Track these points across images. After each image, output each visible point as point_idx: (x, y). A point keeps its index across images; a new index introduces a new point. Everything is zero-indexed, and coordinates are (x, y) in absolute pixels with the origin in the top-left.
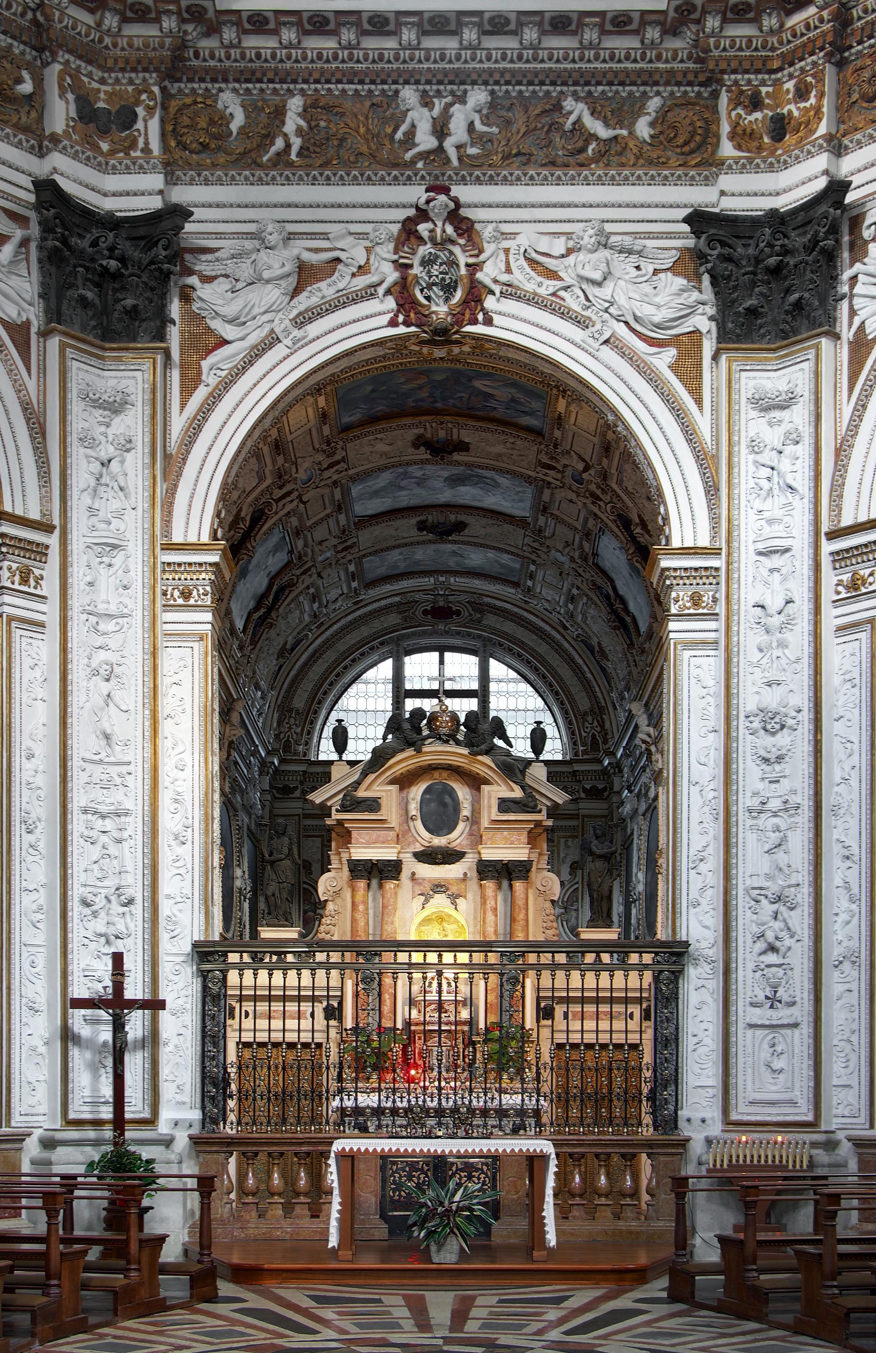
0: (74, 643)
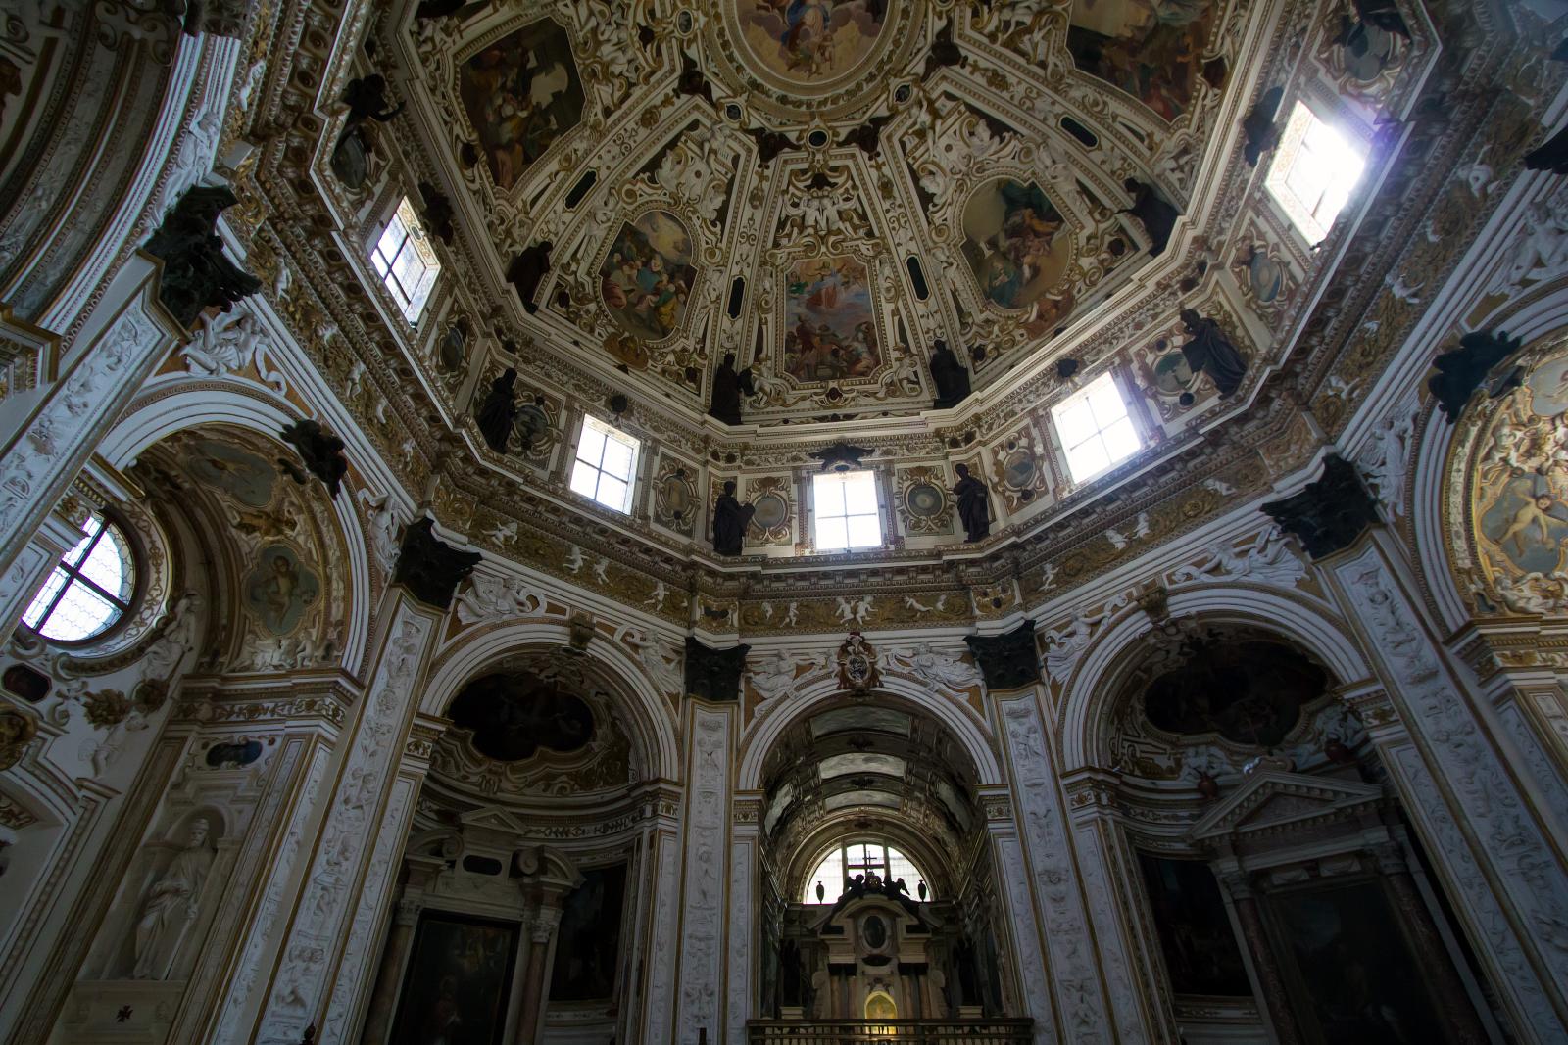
0: (690, 843)
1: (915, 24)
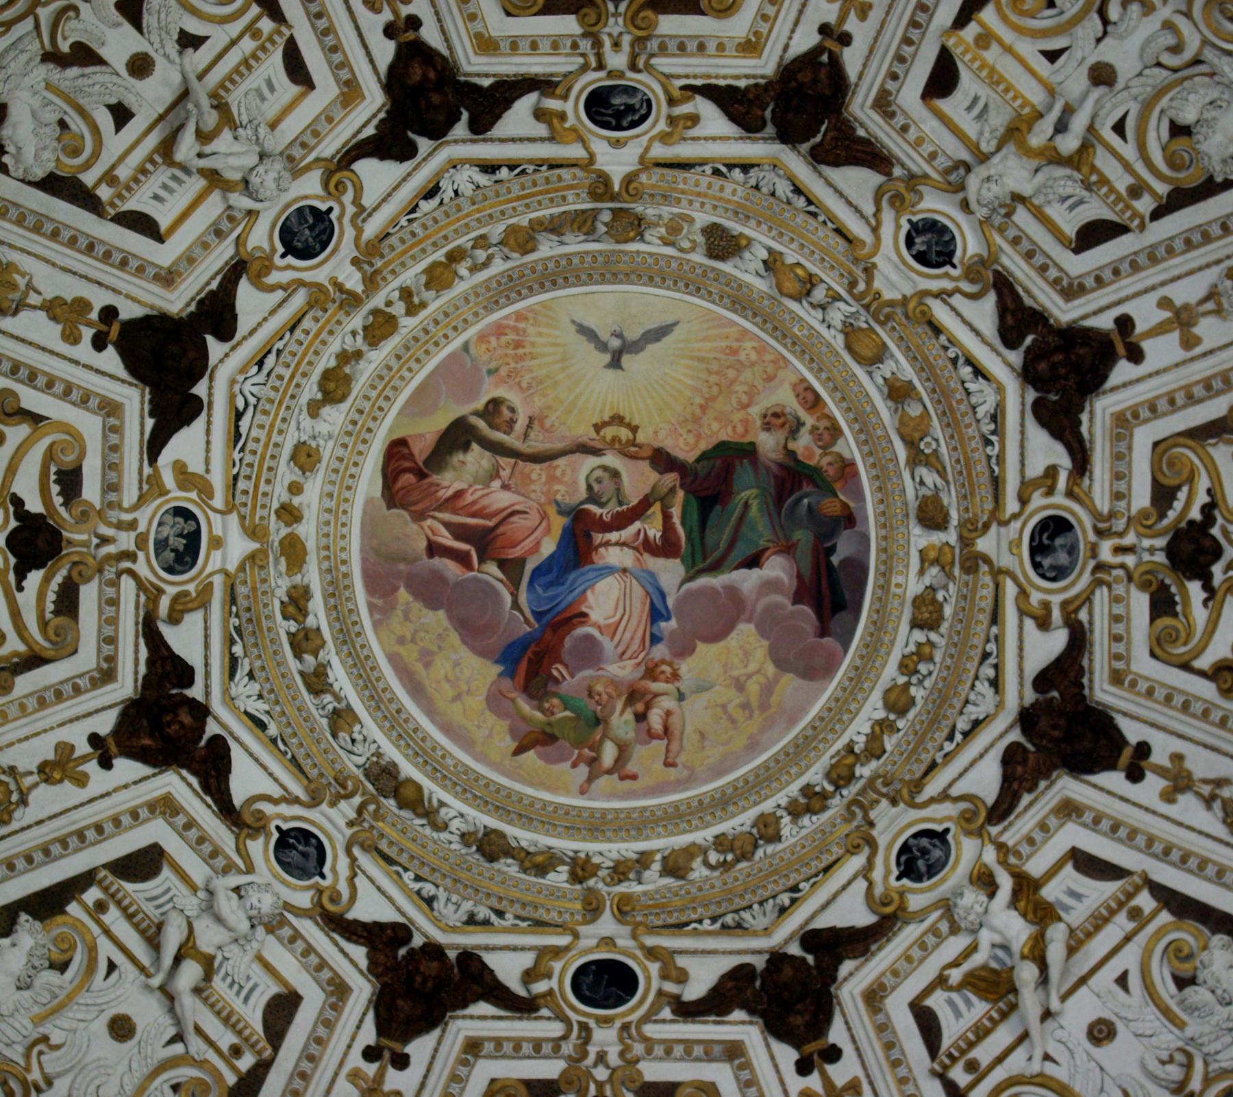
1: (959, 646)
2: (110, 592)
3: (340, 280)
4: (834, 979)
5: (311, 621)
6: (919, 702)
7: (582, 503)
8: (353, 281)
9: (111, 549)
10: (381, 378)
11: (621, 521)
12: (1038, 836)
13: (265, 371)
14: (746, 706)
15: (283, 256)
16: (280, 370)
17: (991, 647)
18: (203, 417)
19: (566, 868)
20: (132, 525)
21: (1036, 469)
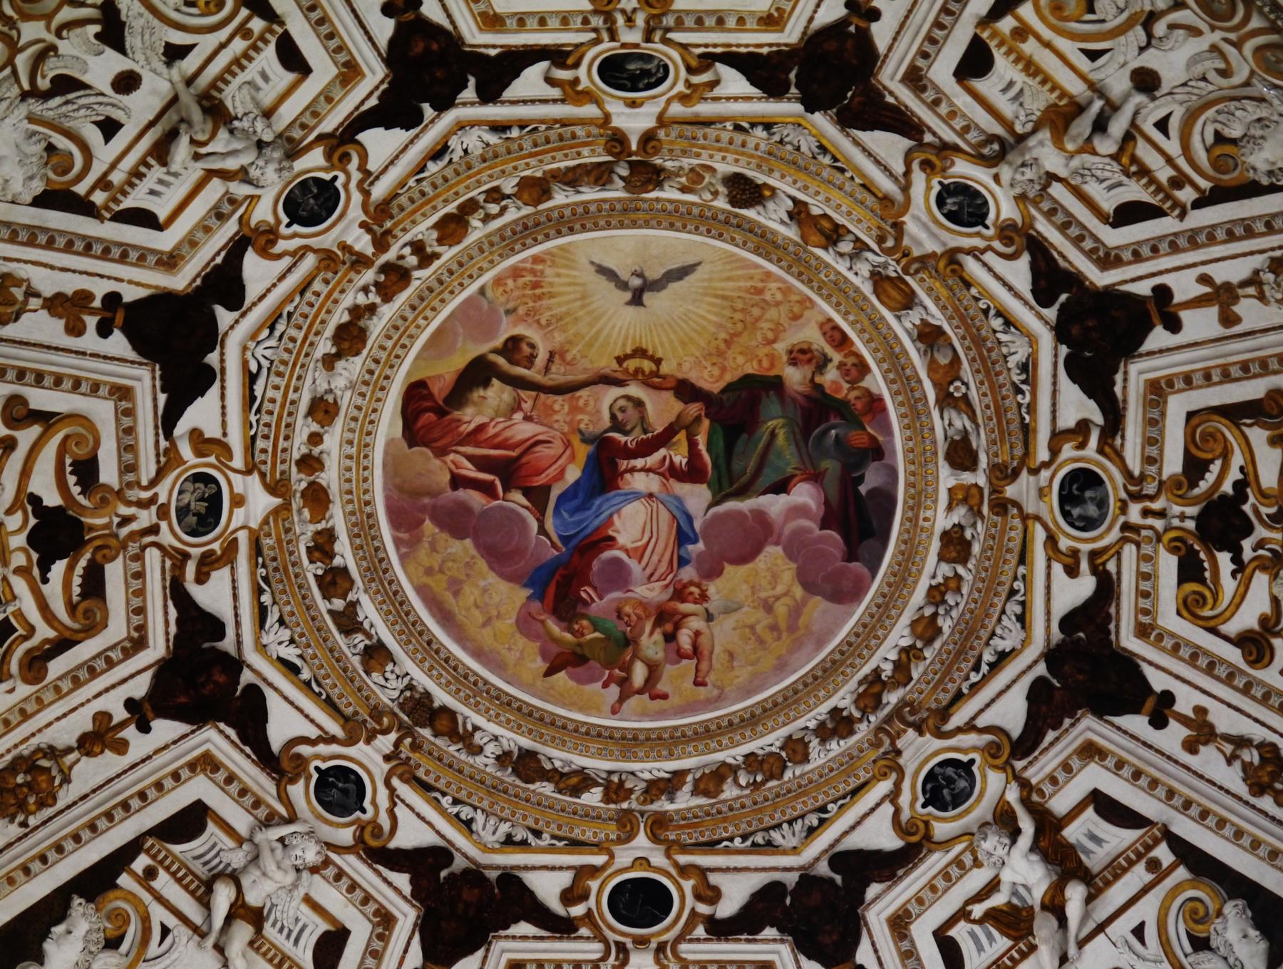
1: (988, 584)
2: (135, 566)
3: (349, 242)
4: (862, 901)
5: (337, 561)
6: (946, 630)
7: (606, 431)
8: (363, 243)
9: (134, 526)
10: (396, 328)
11: (646, 448)
12: (1061, 776)
13: (277, 333)
14: (774, 628)
15: (288, 225)
16: (292, 332)
17: (1018, 585)
18: (217, 384)
19: (601, 789)
20: (153, 500)
21: (1068, 420)
